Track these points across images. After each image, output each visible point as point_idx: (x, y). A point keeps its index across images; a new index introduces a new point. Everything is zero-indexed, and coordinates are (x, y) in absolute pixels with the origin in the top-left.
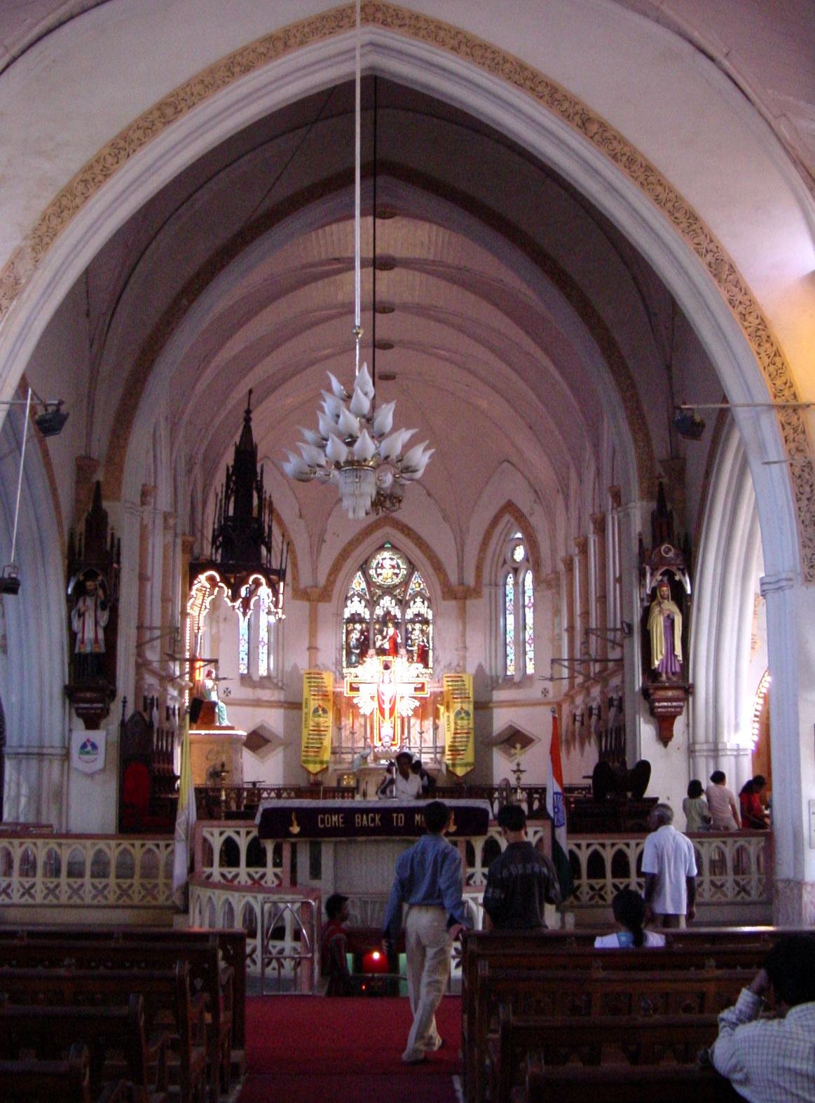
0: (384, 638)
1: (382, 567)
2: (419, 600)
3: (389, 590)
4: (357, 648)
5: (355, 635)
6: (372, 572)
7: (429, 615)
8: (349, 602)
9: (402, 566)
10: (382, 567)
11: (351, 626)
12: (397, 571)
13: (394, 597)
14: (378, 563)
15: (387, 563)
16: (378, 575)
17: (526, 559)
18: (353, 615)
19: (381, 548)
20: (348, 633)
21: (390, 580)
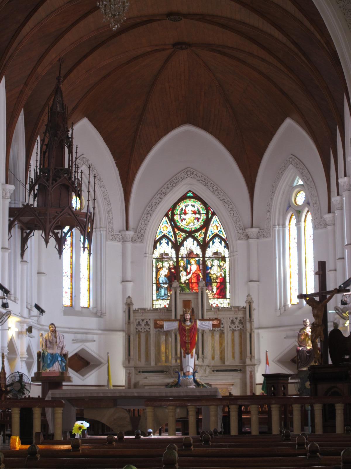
0: (188, 273)
1: (185, 213)
2: (217, 240)
3: (190, 234)
4: (165, 283)
5: (164, 272)
6: (177, 217)
7: (225, 253)
8: (158, 244)
9: (202, 212)
10: (185, 213)
11: (160, 265)
12: (198, 216)
13: (195, 239)
14: (182, 209)
15: (189, 209)
16: (182, 220)
17: (307, 203)
18: (161, 255)
19: (184, 197)
20: (158, 270)
21: (192, 224)
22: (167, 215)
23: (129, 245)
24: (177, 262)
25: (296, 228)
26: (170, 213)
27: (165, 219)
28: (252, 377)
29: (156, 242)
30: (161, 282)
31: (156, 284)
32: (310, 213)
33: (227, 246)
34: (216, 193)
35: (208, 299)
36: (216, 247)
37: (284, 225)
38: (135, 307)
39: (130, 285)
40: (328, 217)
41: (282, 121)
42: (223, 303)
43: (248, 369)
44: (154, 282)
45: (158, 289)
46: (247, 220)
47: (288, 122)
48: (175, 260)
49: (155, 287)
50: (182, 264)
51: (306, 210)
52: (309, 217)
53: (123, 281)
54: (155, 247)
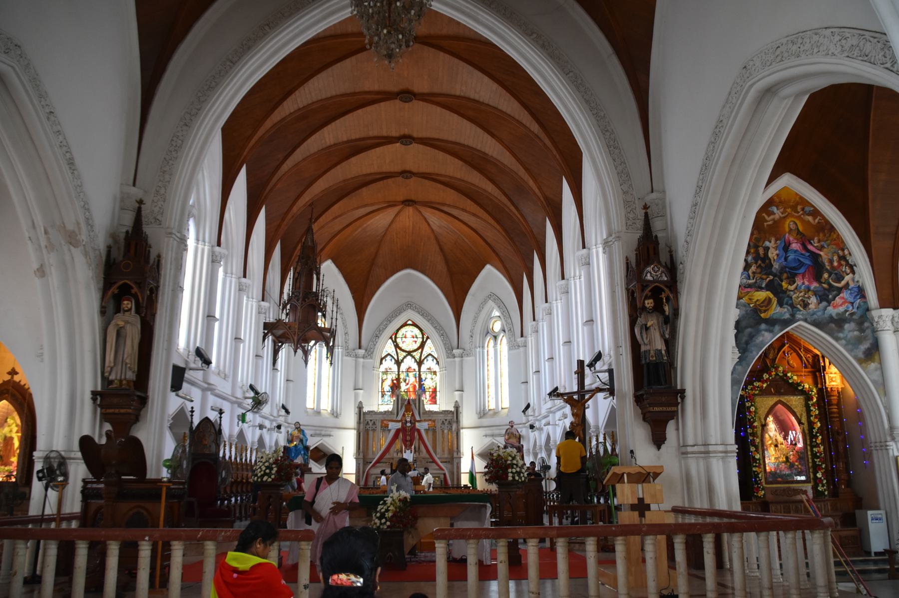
4: (389, 391)
7: (436, 368)
11: (385, 377)
12: (415, 339)
18: (386, 369)
20: (383, 381)
22: (391, 338)
23: (361, 360)
24: (399, 375)
25: (493, 349)
26: (393, 337)
27: (390, 341)
28: (459, 468)
29: (382, 359)
30: (385, 390)
31: (382, 392)
32: (504, 337)
33: (438, 363)
34: (430, 321)
35: (424, 405)
36: (429, 363)
37: (483, 347)
38: (365, 410)
39: (361, 391)
40: (520, 340)
41: (483, 267)
42: (434, 408)
43: (455, 461)
44: (380, 390)
45: (383, 396)
46: (455, 344)
47: (488, 267)
48: (397, 373)
49: (380, 393)
50: (402, 376)
51: (502, 335)
52: (505, 340)
53: (355, 389)
54: (381, 363)
